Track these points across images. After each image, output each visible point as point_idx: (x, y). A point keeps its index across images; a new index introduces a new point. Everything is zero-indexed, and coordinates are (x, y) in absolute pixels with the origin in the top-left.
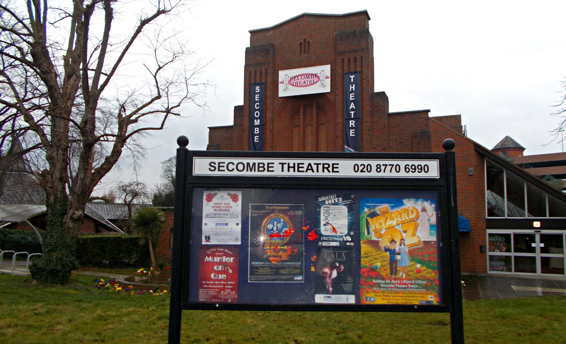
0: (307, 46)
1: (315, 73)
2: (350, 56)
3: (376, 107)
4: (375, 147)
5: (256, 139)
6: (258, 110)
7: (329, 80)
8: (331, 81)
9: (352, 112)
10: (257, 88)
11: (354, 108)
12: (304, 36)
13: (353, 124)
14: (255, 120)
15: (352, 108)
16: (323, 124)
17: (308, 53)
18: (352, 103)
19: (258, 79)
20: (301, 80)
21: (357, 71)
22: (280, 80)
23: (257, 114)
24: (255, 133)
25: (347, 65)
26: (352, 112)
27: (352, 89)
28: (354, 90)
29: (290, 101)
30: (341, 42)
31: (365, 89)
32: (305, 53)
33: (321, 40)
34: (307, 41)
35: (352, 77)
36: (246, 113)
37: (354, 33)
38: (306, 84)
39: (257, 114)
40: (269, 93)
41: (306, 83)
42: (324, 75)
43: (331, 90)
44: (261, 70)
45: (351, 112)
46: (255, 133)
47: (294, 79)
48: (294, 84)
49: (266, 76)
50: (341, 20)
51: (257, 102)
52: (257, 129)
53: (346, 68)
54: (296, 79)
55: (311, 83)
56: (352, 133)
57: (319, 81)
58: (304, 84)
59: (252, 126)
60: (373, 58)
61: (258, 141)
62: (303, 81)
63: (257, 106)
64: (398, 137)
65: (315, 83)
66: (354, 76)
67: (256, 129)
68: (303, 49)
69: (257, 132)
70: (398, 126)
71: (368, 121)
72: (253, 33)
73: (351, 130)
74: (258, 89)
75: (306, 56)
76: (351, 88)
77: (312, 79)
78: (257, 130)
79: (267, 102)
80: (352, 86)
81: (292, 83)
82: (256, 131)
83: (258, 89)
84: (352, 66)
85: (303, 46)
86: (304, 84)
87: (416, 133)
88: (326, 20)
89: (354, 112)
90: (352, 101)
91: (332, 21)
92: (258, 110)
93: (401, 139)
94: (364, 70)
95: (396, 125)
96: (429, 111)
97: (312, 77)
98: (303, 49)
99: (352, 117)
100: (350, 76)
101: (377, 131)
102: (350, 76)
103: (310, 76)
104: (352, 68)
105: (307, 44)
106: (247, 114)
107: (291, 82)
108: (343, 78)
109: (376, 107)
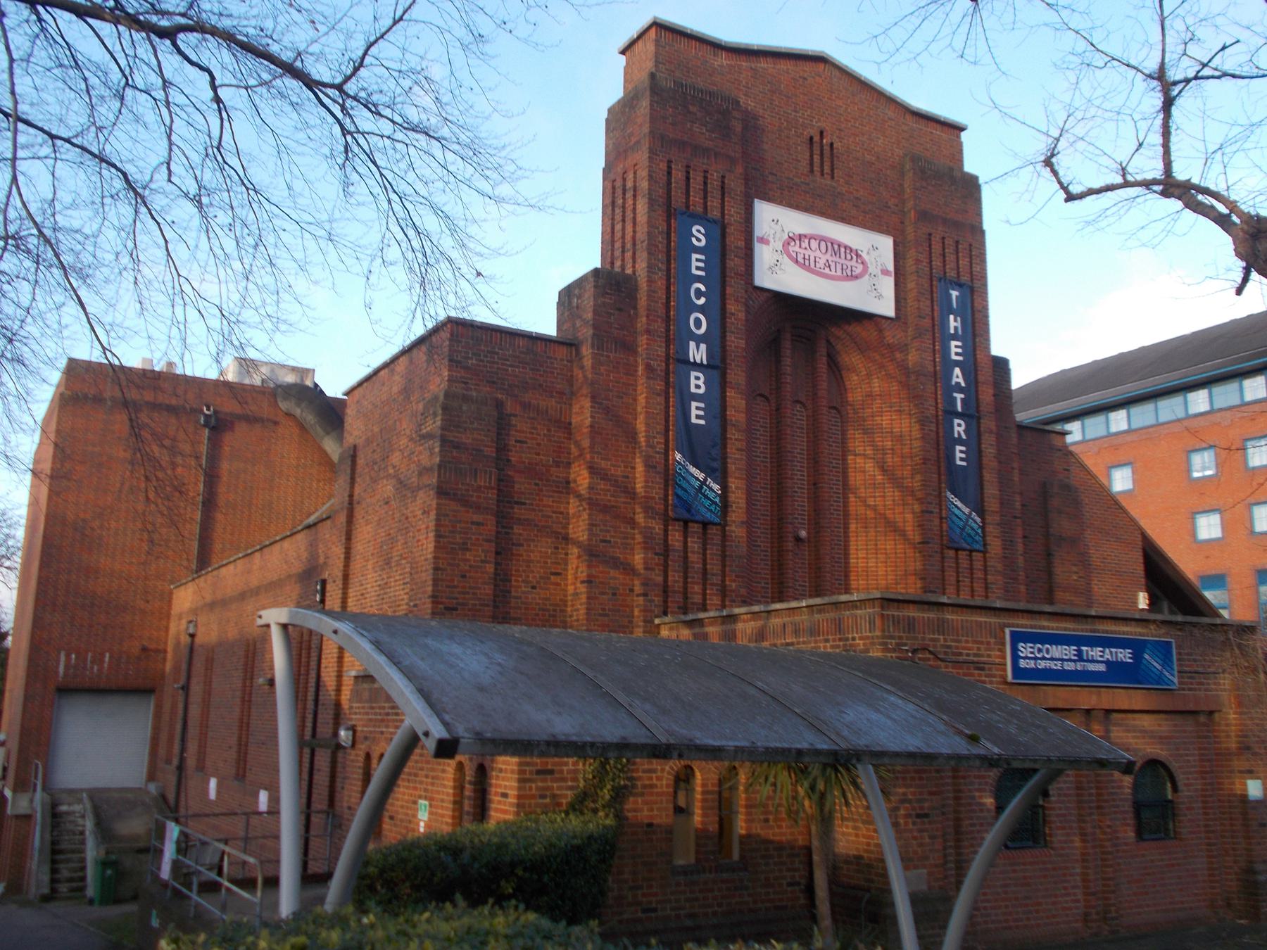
1: (854, 247)
5: (696, 412)
6: (701, 309)
8: (896, 285)
11: (963, 385)
13: (961, 429)
14: (692, 345)
15: (958, 384)
17: (833, 178)
18: (957, 371)
20: (821, 257)
23: (698, 324)
24: (693, 390)
27: (956, 328)
30: (924, 184)
35: (954, 294)
39: (699, 323)
44: (706, 172)
45: (955, 395)
46: (693, 390)
47: (798, 242)
48: (801, 260)
50: (911, 122)
51: (699, 279)
57: (867, 277)
58: (827, 270)
59: (679, 361)
61: (702, 422)
63: (699, 294)
65: (856, 277)
67: (693, 374)
68: (816, 158)
69: (698, 387)
74: (699, 237)
77: (849, 264)
78: (697, 383)
81: (794, 255)
82: (693, 382)
83: (699, 237)
85: (817, 151)
86: (827, 270)
89: (962, 396)
90: (957, 363)
92: (701, 309)
97: (849, 257)
98: (816, 158)
99: (959, 409)
103: (843, 250)
105: (827, 148)
107: (791, 249)
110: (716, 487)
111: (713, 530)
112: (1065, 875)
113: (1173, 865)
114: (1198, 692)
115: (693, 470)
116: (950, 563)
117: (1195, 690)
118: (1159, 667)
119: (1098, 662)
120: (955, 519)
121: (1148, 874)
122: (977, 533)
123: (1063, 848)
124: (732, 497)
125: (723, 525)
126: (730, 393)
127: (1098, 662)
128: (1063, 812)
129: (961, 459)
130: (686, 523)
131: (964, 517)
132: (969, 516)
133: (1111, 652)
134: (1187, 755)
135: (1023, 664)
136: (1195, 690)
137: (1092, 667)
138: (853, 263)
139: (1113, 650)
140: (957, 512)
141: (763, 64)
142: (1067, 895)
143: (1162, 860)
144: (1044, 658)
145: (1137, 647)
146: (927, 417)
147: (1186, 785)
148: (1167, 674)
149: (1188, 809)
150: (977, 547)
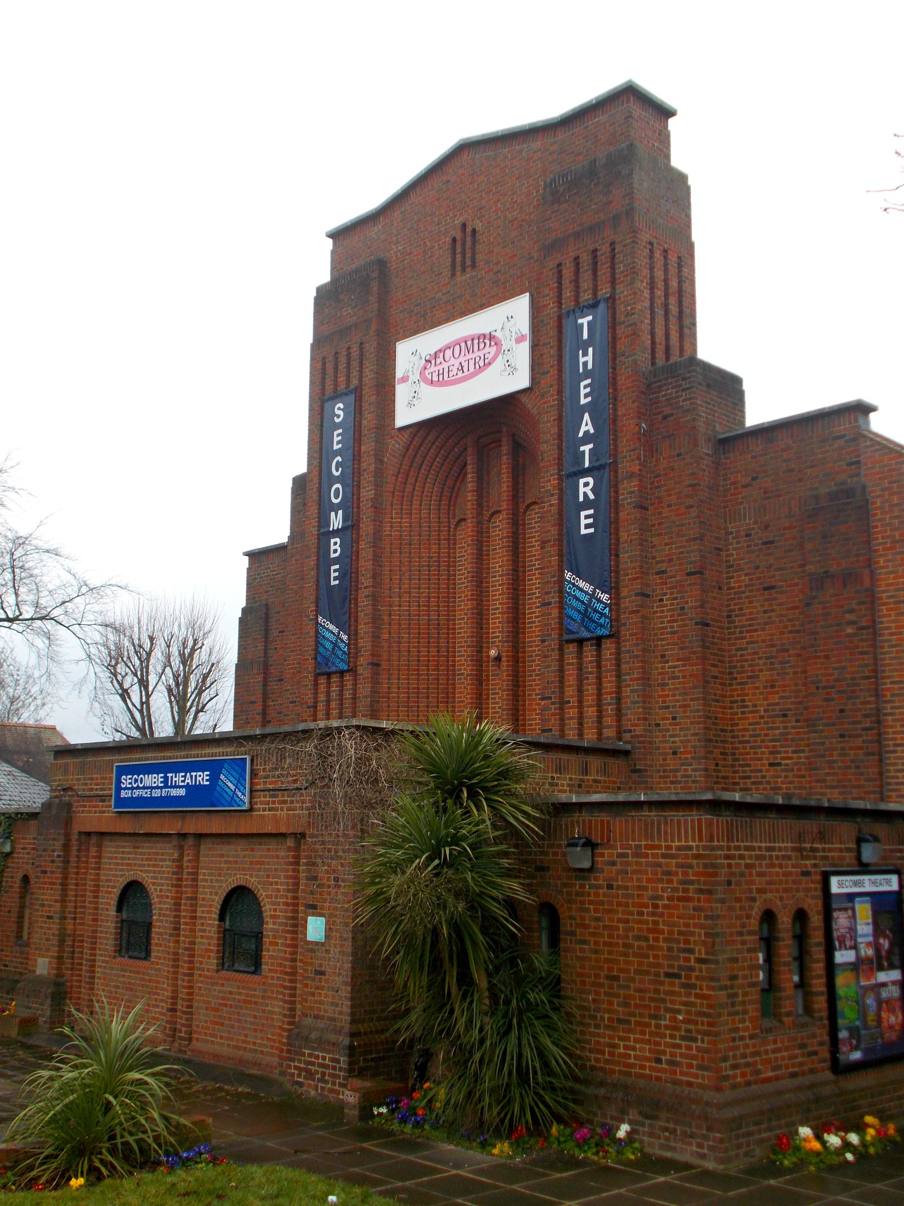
0: (469, 244)
1: (487, 332)
2: (579, 249)
3: (665, 418)
4: (664, 566)
7: (525, 346)
8: (535, 348)
9: (586, 448)
10: (339, 409)
12: (461, 215)
13: (588, 490)
16: (535, 503)
17: (473, 266)
18: (587, 417)
19: (342, 379)
21: (599, 298)
22: (399, 374)
25: (570, 283)
26: (586, 448)
28: (590, 366)
29: (431, 437)
30: (556, 207)
31: (623, 358)
32: (464, 270)
33: (505, 216)
34: (469, 230)
35: (584, 321)
36: (313, 488)
37: (592, 171)
38: (466, 373)
40: (369, 420)
41: (465, 369)
42: (513, 334)
43: (533, 378)
45: (582, 448)
46: (333, 555)
47: (433, 362)
48: (435, 379)
49: (361, 363)
50: (562, 136)
52: (335, 544)
53: (568, 294)
54: (438, 361)
55: (477, 367)
56: (585, 522)
58: (460, 374)
60: (690, 247)
62: (457, 365)
63: (338, 465)
64: (755, 523)
65: (490, 364)
66: (590, 318)
70: (753, 479)
71: (632, 475)
72: (337, 235)
73: (583, 514)
75: (466, 280)
76: (582, 360)
77: (481, 354)
78: (335, 546)
79: (363, 448)
80: (585, 354)
82: (333, 548)
84: (586, 283)
85: (459, 250)
86: (460, 374)
87: (817, 498)
88: (518, 148)
89: (591, 446)
91: (536, 144)
93: (766, 527)
94: (620, 288)
95: (749, 478)
96: (862, 409)
97: (482, 345)
99: (587, 465)
100: (580, 321)
101: (669, 506)
102: (580, 321)
103: (476, 341)
104: (585, 291)
106: (315, 497)
107: (427, 372)
108: (560, 328)
109: (665, 418)
110: (345, 637)
111: (348, 677)
112: (157, 988)
113: (250, 1002)
114: (279, 812)
115: (332, 627)
116: (322, 688)
117: (276, 809)
118: (233, 788)
119: (180, 787)
120: (575, 603)
121: (226, 1005)
122: (602, 615)
123: (157, 964)
124: (361, 643)
125: (353, 671)
126: (362, 545)
127: (180, 787)
128: (161, 930)
129: (587, 526)
130: (329, 675)
131: (586, 599)
132: (593, 596)
133: (191, 776)
134: (277, 883)
135: (123, 794)
136: (276, 809)
137: (174, 792)
138: (487, 349)
139: (194, 774)
140: (578, 593)
141: (415, 198)
142: (157, 1006)
143: (240, 994)
144: (138, 788)
145: (215, 768)
146: (548, 491)
147: (272, 916)
148: (239, 794)
149: (272, 943)
150: (605, 632)
